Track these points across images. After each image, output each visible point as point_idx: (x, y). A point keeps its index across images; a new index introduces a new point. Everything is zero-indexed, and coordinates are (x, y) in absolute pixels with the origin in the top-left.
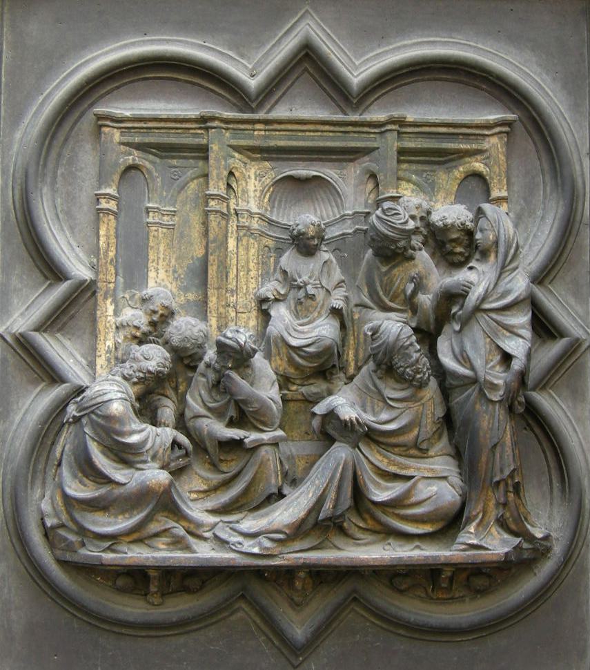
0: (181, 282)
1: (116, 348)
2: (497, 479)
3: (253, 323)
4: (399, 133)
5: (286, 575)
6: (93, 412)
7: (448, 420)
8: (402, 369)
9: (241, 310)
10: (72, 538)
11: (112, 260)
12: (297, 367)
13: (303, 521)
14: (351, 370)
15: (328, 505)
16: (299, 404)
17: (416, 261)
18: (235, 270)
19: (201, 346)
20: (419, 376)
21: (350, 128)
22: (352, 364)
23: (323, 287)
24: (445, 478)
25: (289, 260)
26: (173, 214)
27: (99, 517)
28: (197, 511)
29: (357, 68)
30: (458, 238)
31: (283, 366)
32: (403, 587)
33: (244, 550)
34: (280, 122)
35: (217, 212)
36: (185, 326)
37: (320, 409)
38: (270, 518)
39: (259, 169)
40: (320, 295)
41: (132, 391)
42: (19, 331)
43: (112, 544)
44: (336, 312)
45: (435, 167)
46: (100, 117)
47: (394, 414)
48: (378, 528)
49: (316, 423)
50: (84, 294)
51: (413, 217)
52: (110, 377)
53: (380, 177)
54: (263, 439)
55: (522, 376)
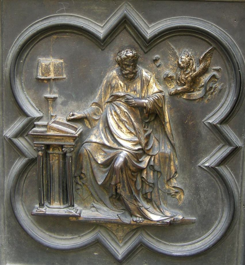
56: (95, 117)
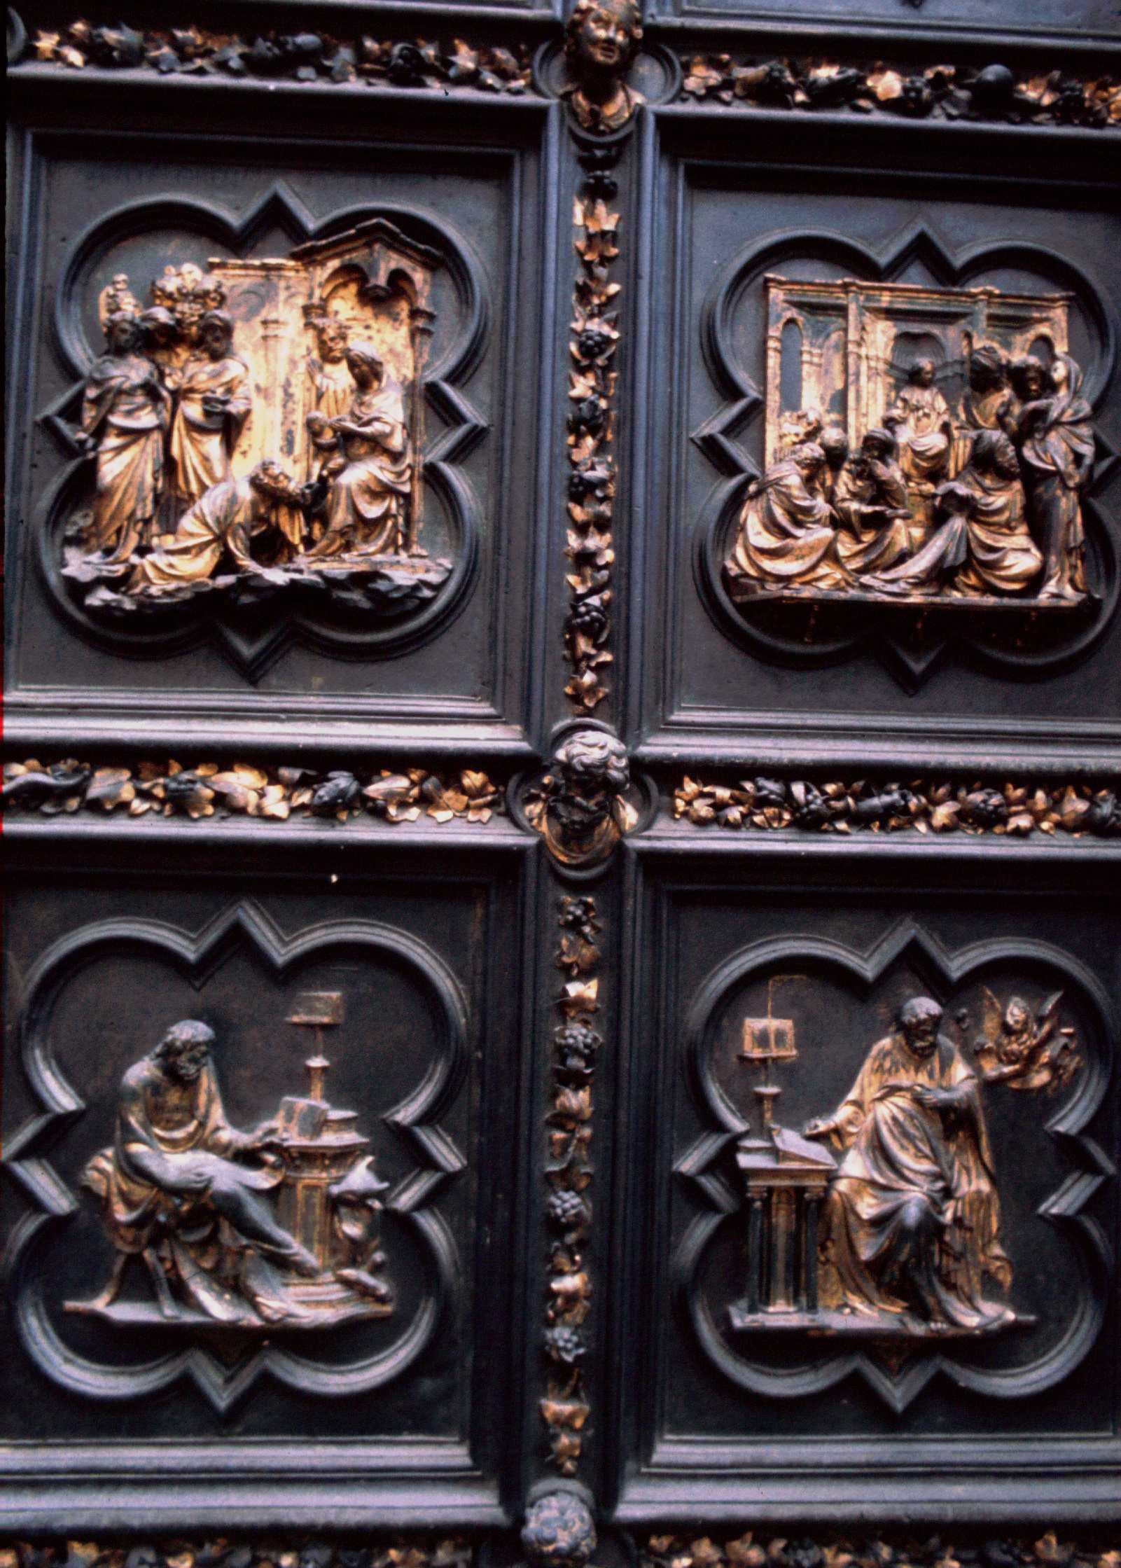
12: (916, 466)
36: (831, 435)
46: (767, 280)
50: (756, 409)
56: (852, 1129)
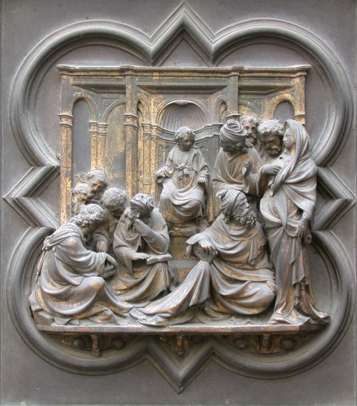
0: (111, 167)
1: (72, 206)
2: (293, 283)
3: (153, 191)
4: (239, 77)
5: (172, 337)
6: (58, 244)
7: (266, 248)
8: (238, 218)
9: (146, 183)
10: (48, 317)
11: (69, 154)
13: (181, 306)
14: (211, 218)
15: (194, 297)
16: (180, 238)
17: (249, 154)
18: (142, 160)
19: (122, 205)
20: (248, 222)
21: (210, 75)
22: (212, 215)
23: (193, 170)
24: (265, 282)
25: (175, 153)
26: (106, 126)
27: (63, 304)
28: (121, 302)
29: (214, 37)
30: (273, 140)
31: (170, 216)
32: (242, 346)
33: (147, 323)
34: (168, 71)
35: (131, 125)
37: (191, 241)
38: (162, 305)
39: (156, 99)
40: (192, 174)
41: (81, 231)
42: (15, 197)
43: (71, 320)
44: (201, 185)
45: (262, 97)
47: (236, 243)
48: (225, 310)
49: (188, 249)
51: (247, 128)
52: (69, 223)
53: (228, 103)
54: (157, 259)
55: (309, 223)
